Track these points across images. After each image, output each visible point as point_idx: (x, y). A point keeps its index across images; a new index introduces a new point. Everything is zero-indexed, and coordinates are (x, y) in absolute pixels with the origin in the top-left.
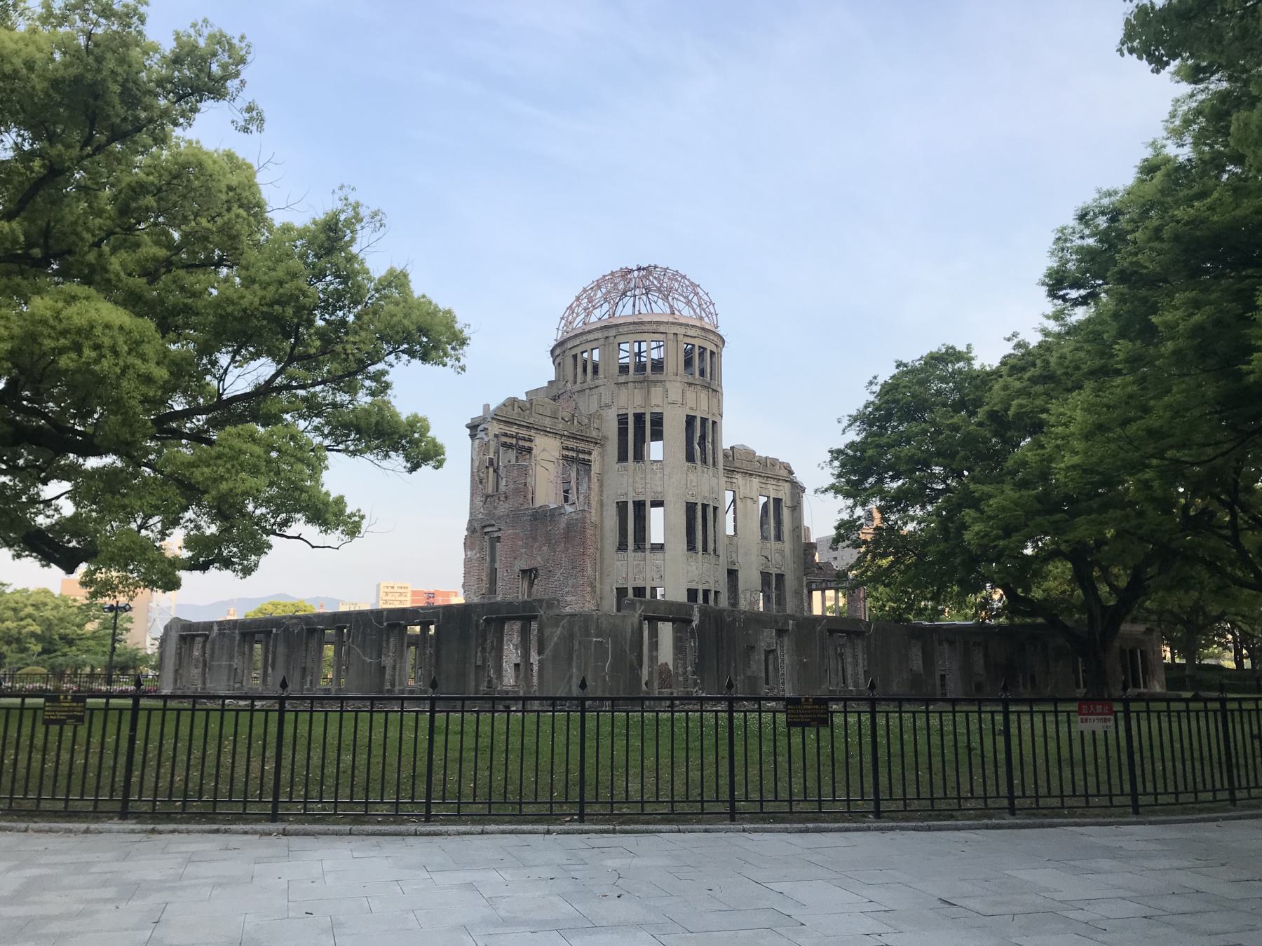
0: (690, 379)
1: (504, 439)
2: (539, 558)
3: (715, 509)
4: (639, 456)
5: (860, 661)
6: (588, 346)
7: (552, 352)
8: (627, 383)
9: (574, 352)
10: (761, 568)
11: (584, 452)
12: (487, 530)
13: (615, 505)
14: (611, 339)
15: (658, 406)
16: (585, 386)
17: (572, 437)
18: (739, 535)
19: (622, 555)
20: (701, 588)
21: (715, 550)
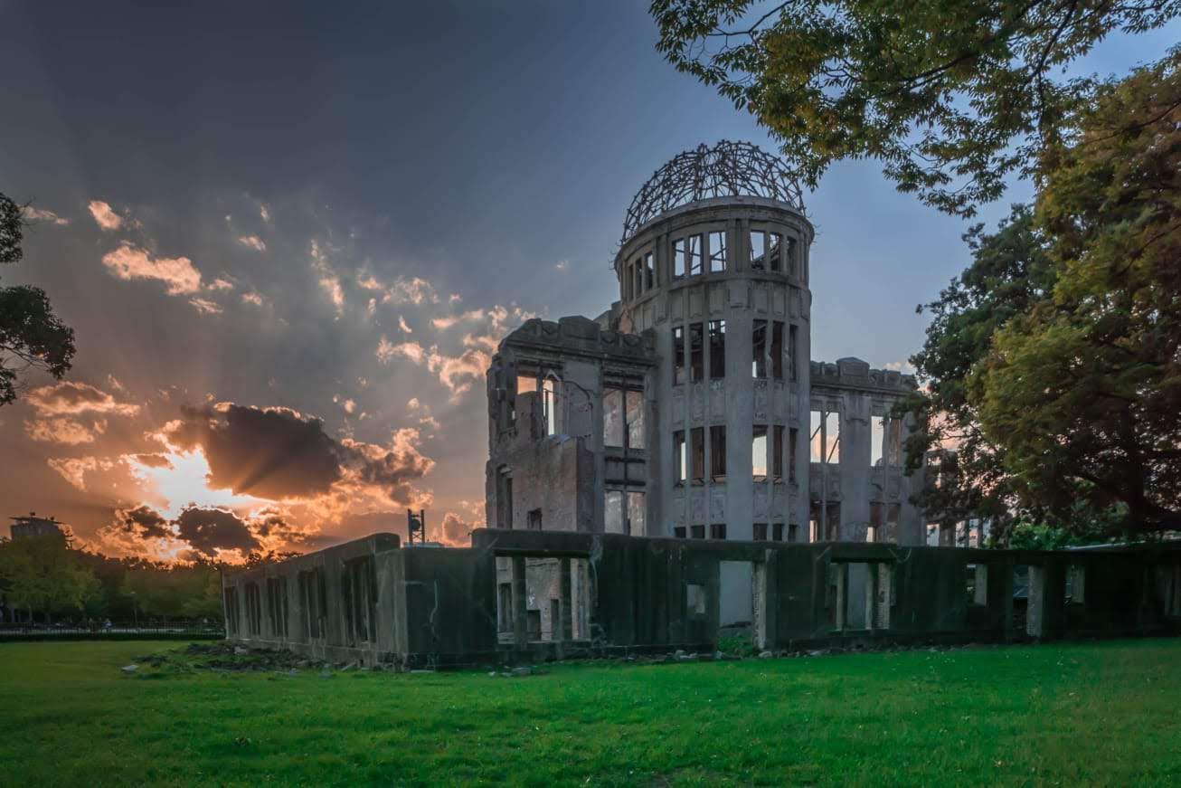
0: (758, 274)
7: (615, 268)
9: (629, 264)
11: (632, 377)
12: (503, 471)
16: (641, 300)
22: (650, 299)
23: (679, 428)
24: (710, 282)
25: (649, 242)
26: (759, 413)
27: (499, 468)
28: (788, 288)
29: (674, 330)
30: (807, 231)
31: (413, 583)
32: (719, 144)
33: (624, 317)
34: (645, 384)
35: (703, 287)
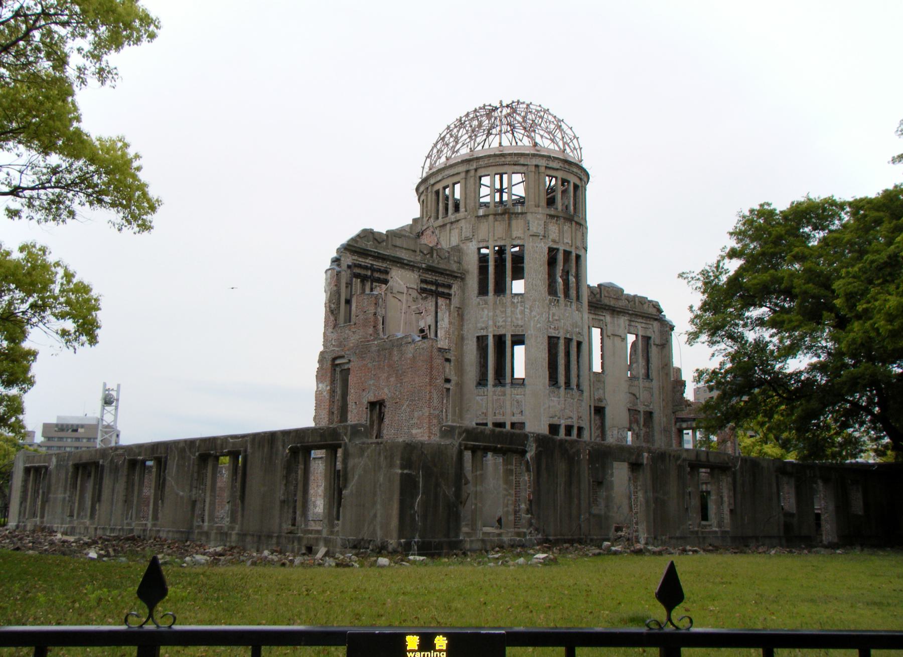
1: (357, 271)
2: (386, 390)
3: (579, 344)
4: (501, 288)
5: (726, 499)
6: (449, 182)
7: (417, 189)
8: (488, 215)
9: (436, 188)
10: (628, 406)
11: (443, 286)
12: (338, 362)
13: (475, 340)
14: (472, 173)
15: (519, 238)
16: (447, 220)
17: (430, 269)
18: (606, 372)
19: (481, 390)
20: (563, 423)
21: (578, 386)
22: (458, 221)
23: (483, 333)
24: (513, 213)
25: (458, 174)
26: (553, 327)
27: (334, 359)
28: (574, 223)
29: (479, 249)
30: (586, 180)
31: (405, 471)
32: (513, 102)
33: (429, 232)
34: (452, 292)
35: (507, 216)
